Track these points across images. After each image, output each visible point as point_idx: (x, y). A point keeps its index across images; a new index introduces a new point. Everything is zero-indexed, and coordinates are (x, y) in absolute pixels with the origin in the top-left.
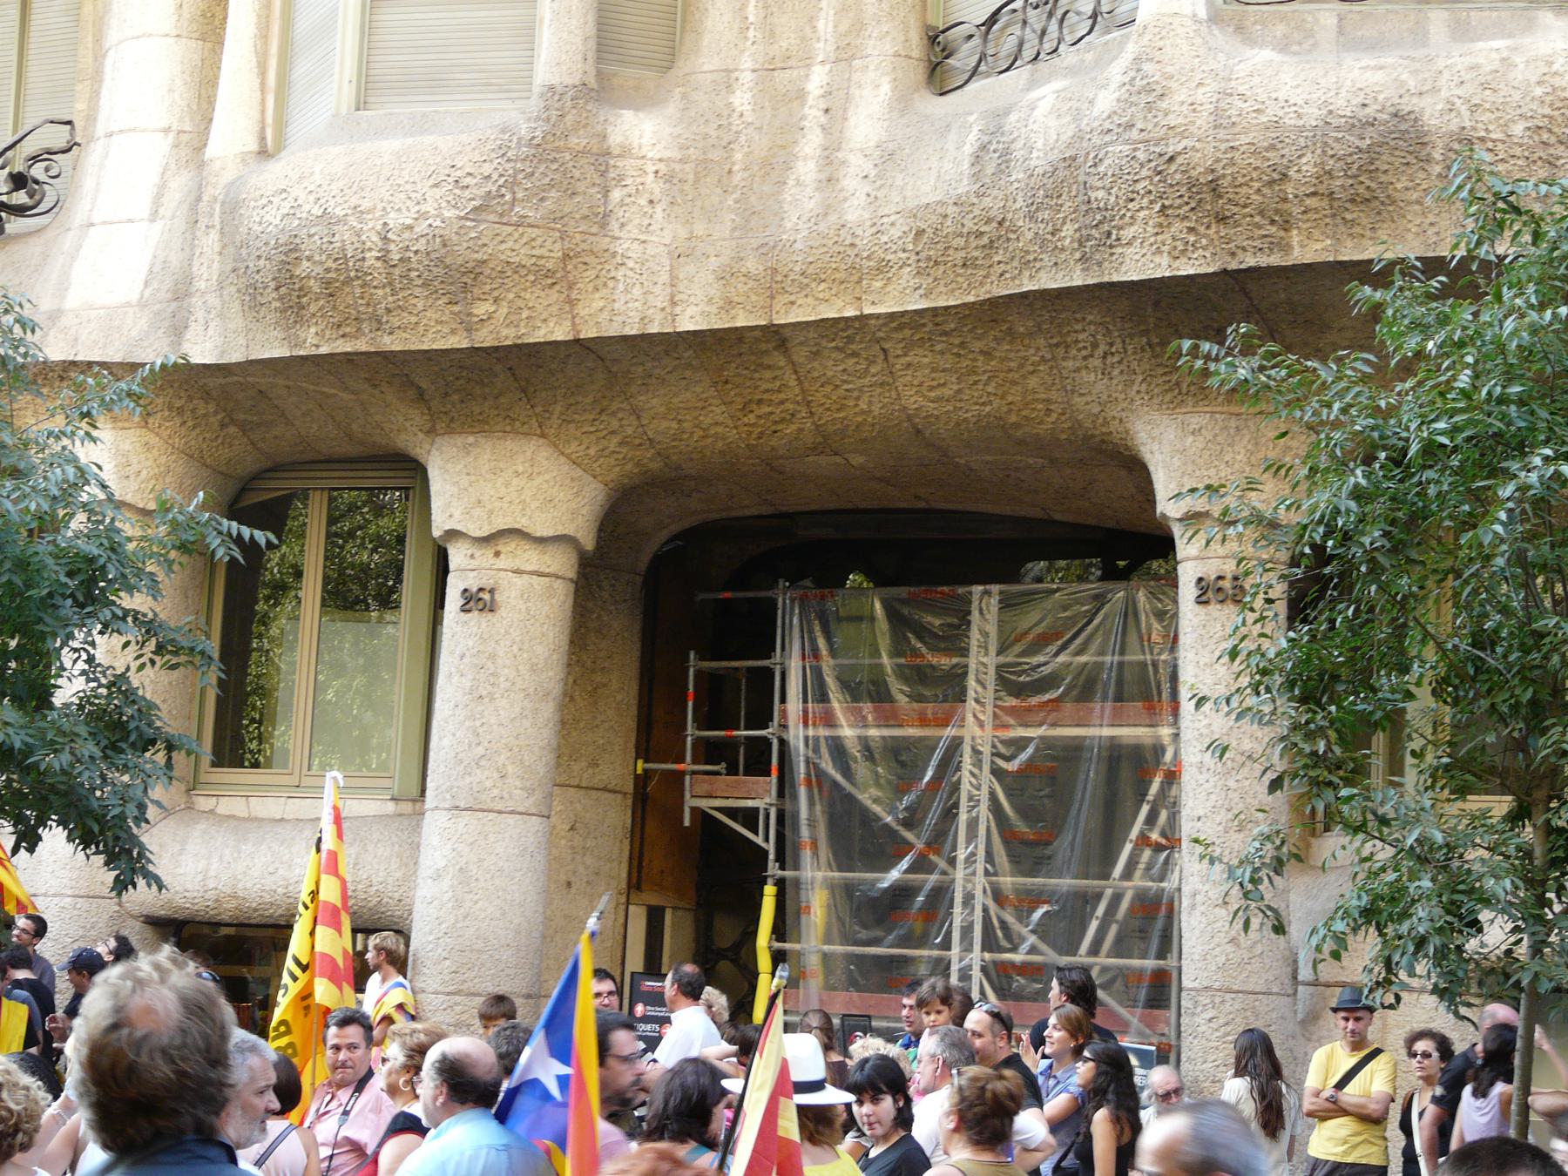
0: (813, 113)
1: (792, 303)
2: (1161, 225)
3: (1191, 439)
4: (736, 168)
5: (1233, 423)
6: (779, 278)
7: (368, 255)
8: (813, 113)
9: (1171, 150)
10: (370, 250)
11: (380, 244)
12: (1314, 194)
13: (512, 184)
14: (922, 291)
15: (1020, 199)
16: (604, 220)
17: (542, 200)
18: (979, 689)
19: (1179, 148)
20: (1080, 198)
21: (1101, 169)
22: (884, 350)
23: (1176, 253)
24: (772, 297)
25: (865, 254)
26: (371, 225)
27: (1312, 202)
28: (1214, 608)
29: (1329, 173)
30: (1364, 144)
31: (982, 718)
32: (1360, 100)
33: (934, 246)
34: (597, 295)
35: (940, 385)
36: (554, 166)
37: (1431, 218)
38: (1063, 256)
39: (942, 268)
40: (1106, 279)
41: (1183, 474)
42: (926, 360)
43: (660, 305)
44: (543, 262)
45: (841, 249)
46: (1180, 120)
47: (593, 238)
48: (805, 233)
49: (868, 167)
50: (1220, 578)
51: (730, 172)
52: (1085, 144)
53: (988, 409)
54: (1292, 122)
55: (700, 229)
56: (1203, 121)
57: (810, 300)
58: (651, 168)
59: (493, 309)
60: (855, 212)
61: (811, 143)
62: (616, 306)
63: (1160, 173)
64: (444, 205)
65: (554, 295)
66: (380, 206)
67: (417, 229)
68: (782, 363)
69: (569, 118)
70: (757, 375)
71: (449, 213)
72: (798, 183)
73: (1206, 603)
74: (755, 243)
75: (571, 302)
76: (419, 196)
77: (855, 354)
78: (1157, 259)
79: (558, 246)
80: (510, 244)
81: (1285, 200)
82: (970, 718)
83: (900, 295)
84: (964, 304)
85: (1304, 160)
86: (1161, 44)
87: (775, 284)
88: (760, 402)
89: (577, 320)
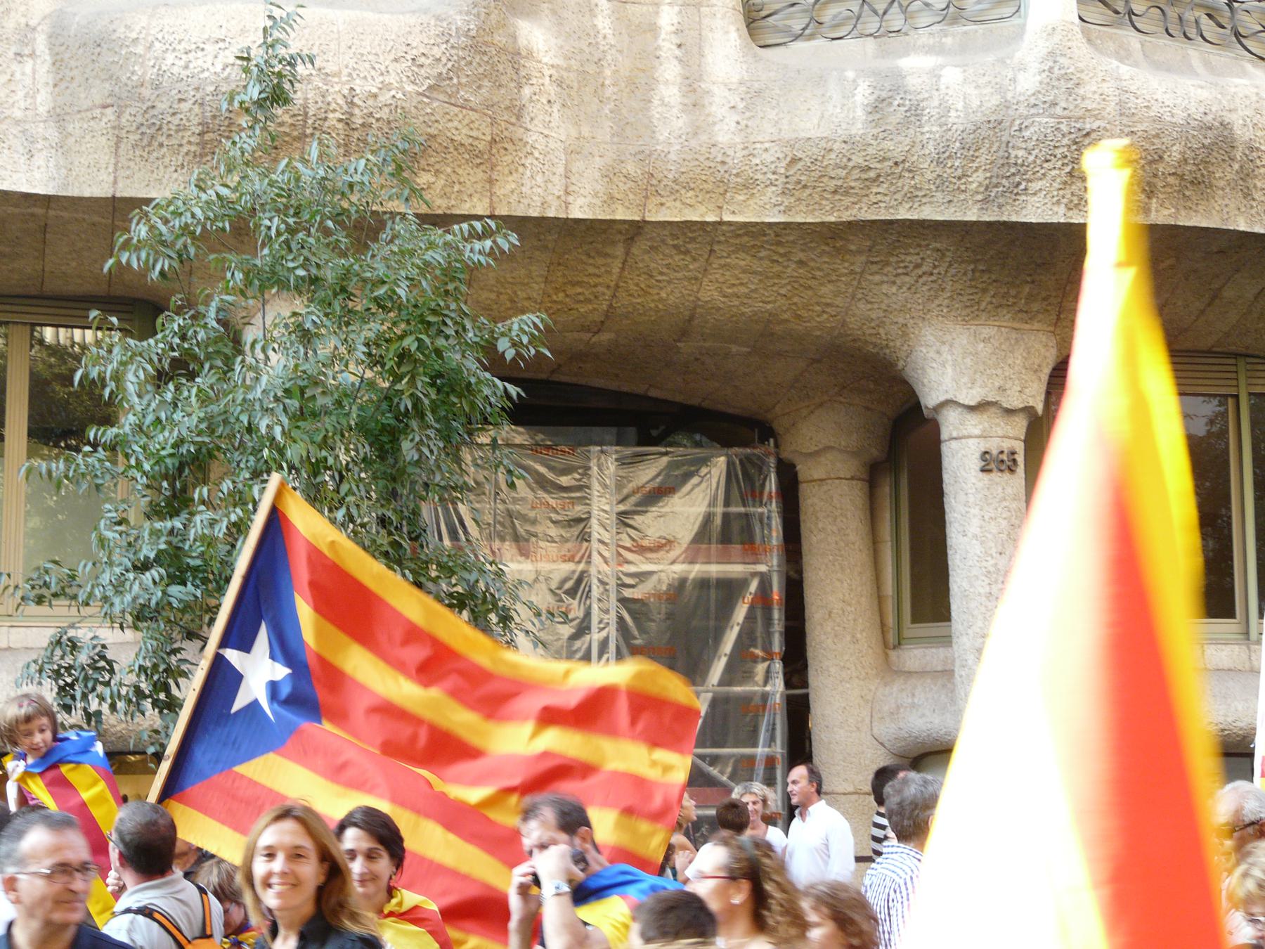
0: (667, 45)
1: (662, 204)
2: (1065, 183)
3: (982, 345)
4: (607, 82)
5: (1014, 335)
6: (654, 182)
7: (331, 115)
8: (667, 45)
9: (1088, 127)
10: (334, 111)
11: (345, 107)
12: (1174, 174)
13: (456, 70)
14: (782, 208)
15: (931, 147)
16: (517, 112)
17: (479, 87)
18: (602, 531)
19: (1095, 126)
20: (1001, 153)
21: (1027, 134)
22: (711, 251)
23: (1071, 205)
24: (646, 197)
25: (735, 172)
26: (337, 88)
27: (1171, 180)
28: (995, 476)
29: (1185, 160)
30: (1207, 142)
31: (606, 554)
32: (1202, 110)
33: (802, 171)
34: (510, 178)
35: (742, 284)
36: (486, 58)
37: (1227, 201)
38: (962, 197)
39: (808, 191)
40: (1005, 218)
41: (975, 372)
42: (742, 263)
43: (557, 194)
44: (476, 143)
45: (712, 165)
46: (1094, 106)
47: (511, 128)
48: (678, 147)
49: (735, 99)
50: (1002, 452)
51: (603, 85)
52: (1011, 112)
53: (769, 307)
54: (1168, 119)
55: (586, 131)
56: (1111, 108)
57: (678, 204)
58: (547, 73)
59: (433, 180)
60: (725, 133)
61: (670, 71)
62: (524, 189)
63: (1076, 143)
64: (405, 79)
65: (480, 175)
66: (345, 72)
67: (381, 98)
68: (618, 253)
69: (493, 16)
70: (591, 261)
71: (409, 88)
72: (663, 104)
73: (990, 471)
74: (632, 150)
75: (491, 181)
76: (383, 68)
77: (687, 252)
78: (1055, 208)
79: (488, 131)
80: (456, 123)
81: (1155, 176)
82: (596, 558)
83: (763, 209)
84: (823, 223)
85: (1174, 148)
86: (1069, 44)
87: (650, 187)
88: (579, 283)
89: (494, 199)
